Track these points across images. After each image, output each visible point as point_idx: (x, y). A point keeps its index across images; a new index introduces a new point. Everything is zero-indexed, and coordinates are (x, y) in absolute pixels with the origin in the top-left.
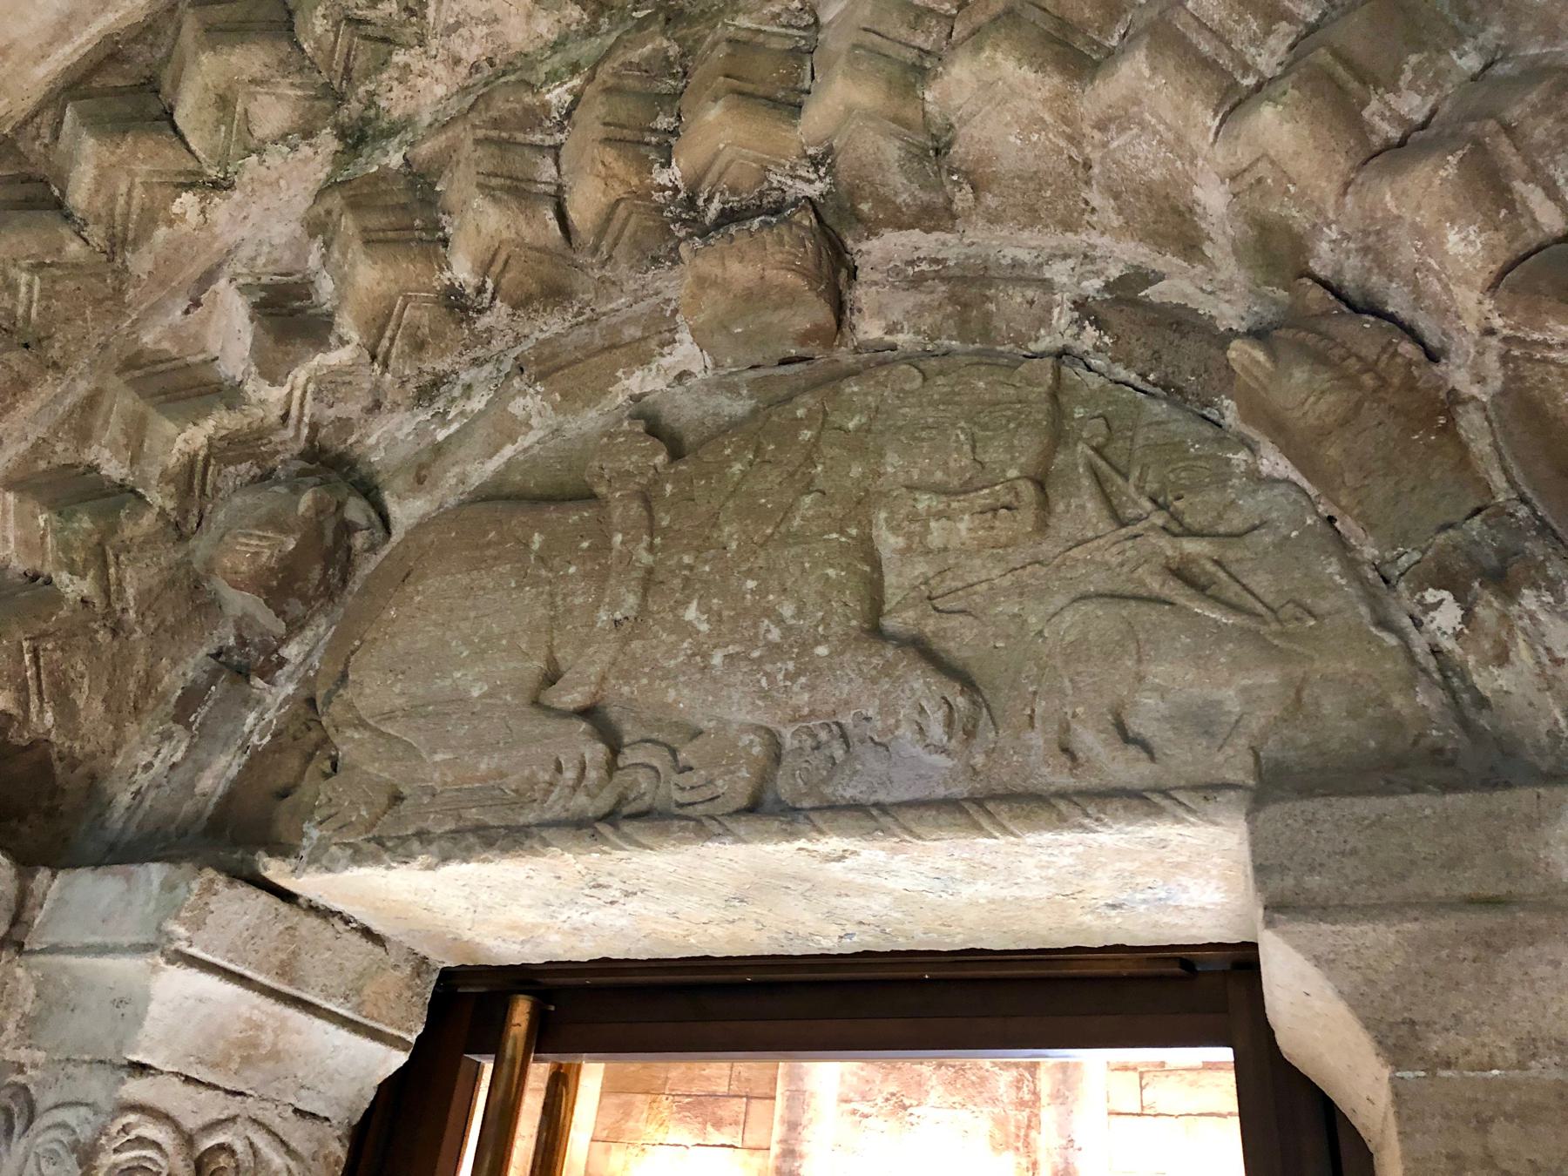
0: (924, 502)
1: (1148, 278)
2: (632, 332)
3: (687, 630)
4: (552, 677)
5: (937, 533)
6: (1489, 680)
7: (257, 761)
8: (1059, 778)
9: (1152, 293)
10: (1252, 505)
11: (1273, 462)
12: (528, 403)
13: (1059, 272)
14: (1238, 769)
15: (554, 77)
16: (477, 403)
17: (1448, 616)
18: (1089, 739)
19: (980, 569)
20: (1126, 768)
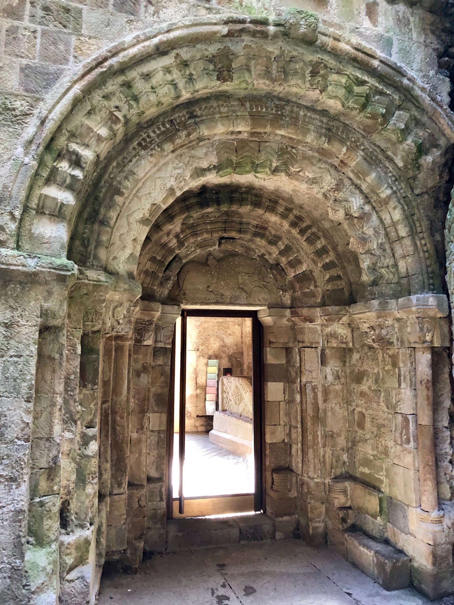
0: (243, 274)
1: (265, 255)
2: (211, 244)
3: (222, 284)
4: (208, 287)
5: (244, 277)
6: (283, 298)
7: (170, 291)
8: (253, 303)
9: (265, 257)
10: (270, 280)
11: (271, 276)
12: (198, 251)
13: (257, 251)
14: (267, 304)
15: (212, 217)
16: (193, 250)
17: (281, 293)
18: (256, 300)
19: (247, 281)
20: (259, 303)
